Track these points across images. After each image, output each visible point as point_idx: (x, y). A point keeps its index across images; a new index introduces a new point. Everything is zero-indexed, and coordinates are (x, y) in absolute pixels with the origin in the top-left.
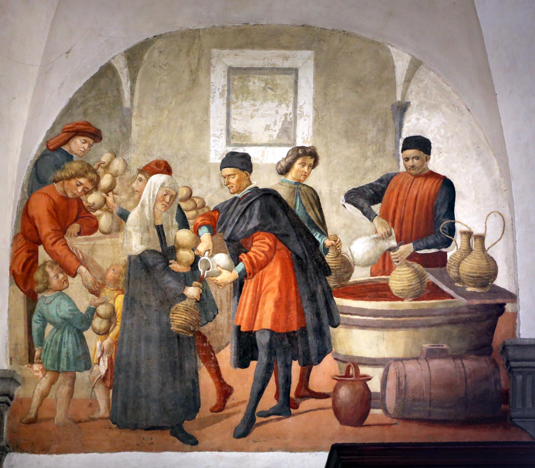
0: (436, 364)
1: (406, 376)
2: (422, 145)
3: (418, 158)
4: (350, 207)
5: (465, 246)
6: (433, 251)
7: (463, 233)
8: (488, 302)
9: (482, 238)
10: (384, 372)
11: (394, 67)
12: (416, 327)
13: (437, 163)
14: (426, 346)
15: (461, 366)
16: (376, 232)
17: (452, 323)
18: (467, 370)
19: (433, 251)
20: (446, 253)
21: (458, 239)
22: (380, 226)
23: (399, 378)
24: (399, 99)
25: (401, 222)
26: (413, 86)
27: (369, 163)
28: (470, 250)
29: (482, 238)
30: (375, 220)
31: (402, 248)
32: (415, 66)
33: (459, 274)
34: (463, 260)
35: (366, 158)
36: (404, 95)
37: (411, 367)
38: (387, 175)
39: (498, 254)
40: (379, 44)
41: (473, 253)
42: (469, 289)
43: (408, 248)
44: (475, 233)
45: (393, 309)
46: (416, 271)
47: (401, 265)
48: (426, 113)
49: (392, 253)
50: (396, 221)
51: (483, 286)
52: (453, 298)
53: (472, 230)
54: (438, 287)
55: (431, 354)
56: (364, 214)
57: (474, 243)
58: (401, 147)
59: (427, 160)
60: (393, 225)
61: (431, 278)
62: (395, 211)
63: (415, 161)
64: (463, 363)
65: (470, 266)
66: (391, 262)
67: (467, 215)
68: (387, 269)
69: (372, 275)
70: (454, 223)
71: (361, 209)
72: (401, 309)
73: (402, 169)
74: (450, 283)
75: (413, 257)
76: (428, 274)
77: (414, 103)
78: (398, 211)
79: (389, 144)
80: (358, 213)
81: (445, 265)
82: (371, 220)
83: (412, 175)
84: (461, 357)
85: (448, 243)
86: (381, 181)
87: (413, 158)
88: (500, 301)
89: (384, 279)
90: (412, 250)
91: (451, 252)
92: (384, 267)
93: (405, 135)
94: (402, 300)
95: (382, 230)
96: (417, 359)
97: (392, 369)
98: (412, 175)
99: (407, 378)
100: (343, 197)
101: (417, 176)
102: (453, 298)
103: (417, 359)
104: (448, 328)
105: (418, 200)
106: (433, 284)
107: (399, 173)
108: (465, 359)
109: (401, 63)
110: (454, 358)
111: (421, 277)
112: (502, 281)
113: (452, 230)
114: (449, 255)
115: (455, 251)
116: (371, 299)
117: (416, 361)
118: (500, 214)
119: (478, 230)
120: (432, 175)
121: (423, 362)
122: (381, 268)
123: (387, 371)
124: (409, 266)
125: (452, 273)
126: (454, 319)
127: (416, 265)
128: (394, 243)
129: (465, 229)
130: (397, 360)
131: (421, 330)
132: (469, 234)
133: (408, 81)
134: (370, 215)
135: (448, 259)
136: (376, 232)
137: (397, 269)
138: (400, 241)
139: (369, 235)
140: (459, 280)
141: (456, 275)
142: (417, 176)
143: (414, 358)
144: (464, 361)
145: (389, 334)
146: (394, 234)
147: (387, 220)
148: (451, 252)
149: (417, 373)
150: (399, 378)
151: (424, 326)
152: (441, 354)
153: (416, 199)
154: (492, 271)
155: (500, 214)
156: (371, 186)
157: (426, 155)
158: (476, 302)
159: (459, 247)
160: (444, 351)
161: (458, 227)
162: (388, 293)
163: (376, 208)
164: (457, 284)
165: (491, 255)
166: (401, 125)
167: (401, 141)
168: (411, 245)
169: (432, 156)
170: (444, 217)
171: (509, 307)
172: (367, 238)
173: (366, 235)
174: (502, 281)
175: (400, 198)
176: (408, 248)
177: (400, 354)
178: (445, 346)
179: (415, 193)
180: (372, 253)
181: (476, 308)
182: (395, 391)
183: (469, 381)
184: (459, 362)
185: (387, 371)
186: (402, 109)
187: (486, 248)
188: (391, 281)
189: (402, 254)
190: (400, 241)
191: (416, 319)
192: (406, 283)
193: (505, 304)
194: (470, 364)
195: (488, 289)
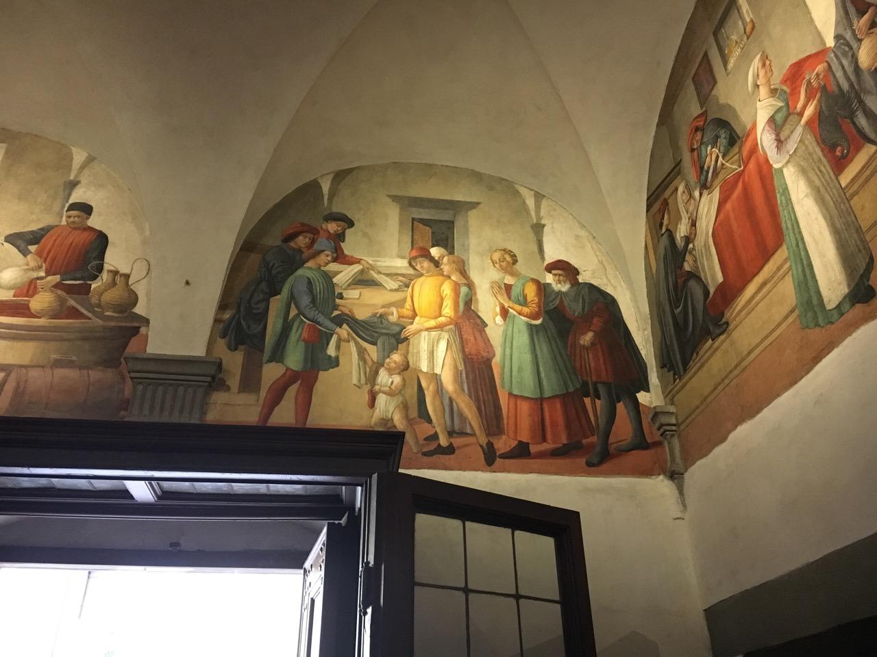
0: (60, 372)
1: (26, 381)
2: (86, 209)
3: (79, 217)
4: (7, 245)
5: (110, 279)
6: (78, 282)
7: (110, 271)
8: (124, 324)
9: (127, 277)
10: (4, 376)
11: (72, 159)
12: (47, 340)
13: (94, 222)
14: (54, 356)
15: (86, 375)
16: (28, 265)
17: (84, 339)
18: (91, 379)
19: (78, 282)
20: (91, 285)
21: (105, 276)
22: (32, 260)
23: (18, 383)
24: (72, 178)
25: (54, 259)
26: (86, 172)
27: (34, 217)
28: (114, 284)
29: (127, 277)
30: (29, 257)
31: (49, 278)
32: (90, 160)
33: (100, 301)
34: (106, 291)
35: (32, 213)
36: (76, 176)
37: (34, 373)
38: (49, 226)
39: (141, 290)
40: (63, 144)
41: (117, 286)
42: (107, 313)
43: (56, 278)
44: (121, 272)
45: (30, 324)
46: (59, 296)
47: (45, 291)
48: (93, 189)
49: (38, 281)
50: (49, 259)
51: (121, 312)
52: (90, 319)
53: (119, 270)
54: (77, 310)
55: (58, 364)
56: (20, 251)
57: (118, 279)
58: (66, 209)
59: (87, 219)
60: (45, 261)
61: (72, 302)
62: (49, 252)
63: (76, 219)
64: (88, 374)
65: (111, 296)
66: (35, 287)
67: (114, 259)
68: (31, 292)
69: (14, 296)
70: (103, 264)
71: (18, 247)
72: (39, 324)
73: (64, 222)
74: (90, 308)
75: (57, 286)
76: (70, 299)
77: (84, 181)
78: (52, 252)
79: (57, 206)
80: (15, 250)
81: (88, 294)
82: (25, 255)
83: (71, 227)
84: (88, 368)
85: (95, 278)
86: (42, 229)
87: (75, 217)
88: (136, 324)
89: (26, 300)
90: (58, 280)
91: (94, 285)
92: (28, 291)
93: (71, 201)
94: (40, 318)
95: (33, 264)
96: (43, 367)
97: (13, 376)
98: (71, 227)
99: (28, 383)
100: (3, 238)
101: (75, 229)
102: (90, 319)
103: (43, 367)
104: (80, 343)
105: (73, 245)
106: (73, 307)
107: (59, 226)
108: (91, 369)
109: (79, 157)
110: (81, 368)
111: (62, 302)
112: (139, 309)
113: (100, 269)
114: (93, 286)
115: (100, 283)
116: (8, 315)
117: (41, 368)
118: (146, 260)
119: (124, 270)
120: (91, 229)
121: (48, 371)
122: (25, 292)
123: (8, 375)
124: (52, 291)
125: (94, 300)
126: (86, 336)
127: (59, 292)
128: (42, 274)
129: (112, 268)
130: (21, 366)
131: (52, 343)
132: (115, 273)
133: (83, 167)
134: (25, 253)
135: (92, 289)
136: (28, 265)
137: (41, 293)
138: (48, 273)
139: (20, 266)
140: (99, 306)
141: (97, 302)
142: (75, 229)
143: (39, 366)
144: (90, 371)
145: (18, 345)
146: (44, 268)
147: (41, 257)
148: (94, 285)
149: (38, 379)
150: (19, 383)
151: (56, 340)
152: (69, 364)
153: (71, 244)
154: (134, 300)
155: (146, 260)
156: (32, 232)
157: (86, 216)
158: (113, 324)
159: (104, 281)
160: (71, 361)
161: (106, 267)
162: (27, 311)
163: (33, 248)
164: (96, 309)
165: (134, 289)
166: (70, 195)
167: (67, 205)
168: (59, 276)
169: (91, 217)
170: (95, 259)
171: (143, 330)
172: (18, 268)
173: (16, 266)
174: (139, 309)
175: (57, 242)
176: (56, 278)
177: (26, 361)
178: (74, 358)
179: (71, 240)
180: (19, 280)
181: (112, 329)
182: (11, 395)
183: (91, 389)
184: (85, 372)
185: (8, 375)
186: (73, 185)
187: (130, 284)
188: (32, 302)
189: (48, 282)
190: (48, 273)
191: (49, 333)
192: (46, 305)
193: (140, 327)
194: (96, 375)
195: (126, 315)
